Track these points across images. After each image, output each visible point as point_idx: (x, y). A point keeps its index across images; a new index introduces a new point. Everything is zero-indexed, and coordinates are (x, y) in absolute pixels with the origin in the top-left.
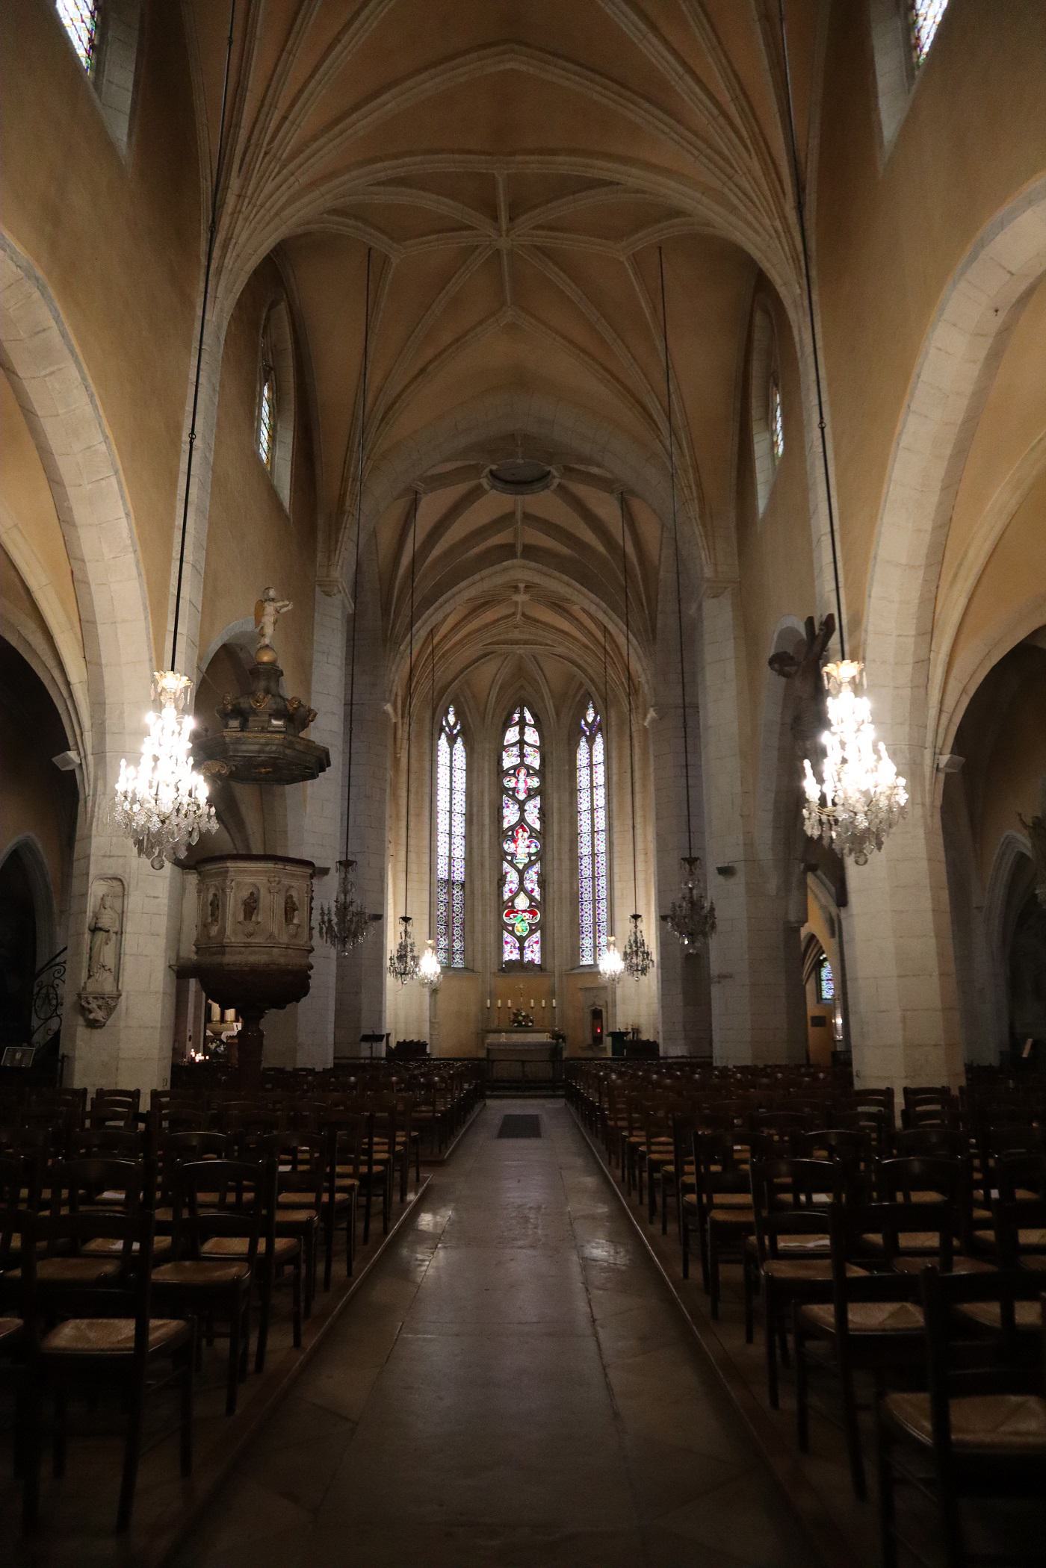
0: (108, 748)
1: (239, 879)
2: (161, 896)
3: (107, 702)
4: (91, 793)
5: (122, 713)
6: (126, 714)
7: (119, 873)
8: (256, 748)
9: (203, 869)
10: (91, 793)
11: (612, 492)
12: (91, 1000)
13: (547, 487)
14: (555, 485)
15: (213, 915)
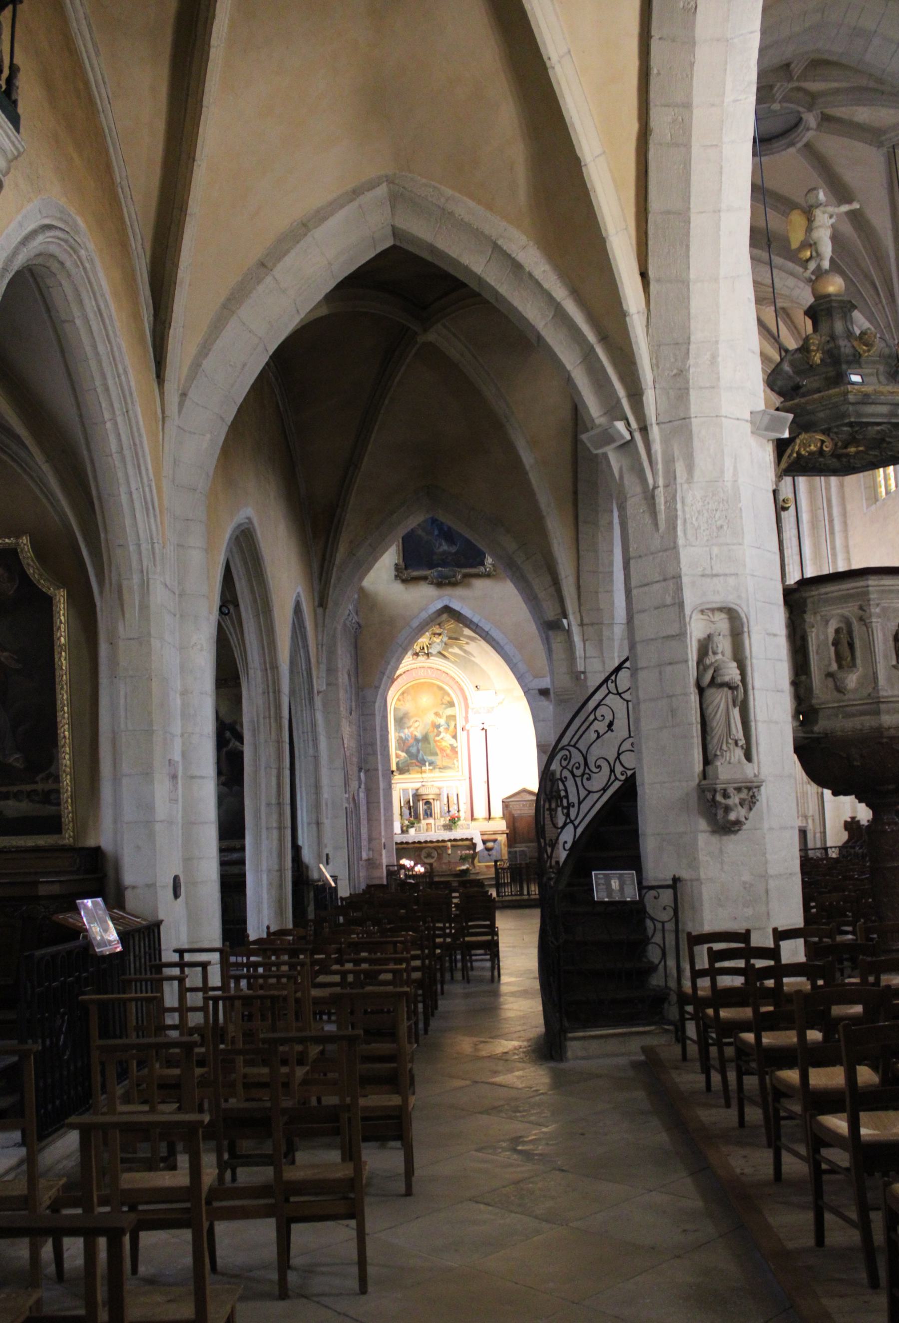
0: (694, 409)
1: (885, 603)
2: (778, 633)
3: (692, 338)
4: (661, 482)
5: (714, 358)
6: (720, 359)
7: (731, 600)
8: (884, 409)
9: (807, 594)
10: (661, 482)
11: (880, 145)
12: (731, 791)
13: (792, 144)
14: (805, 140)
15: (839, 658)
